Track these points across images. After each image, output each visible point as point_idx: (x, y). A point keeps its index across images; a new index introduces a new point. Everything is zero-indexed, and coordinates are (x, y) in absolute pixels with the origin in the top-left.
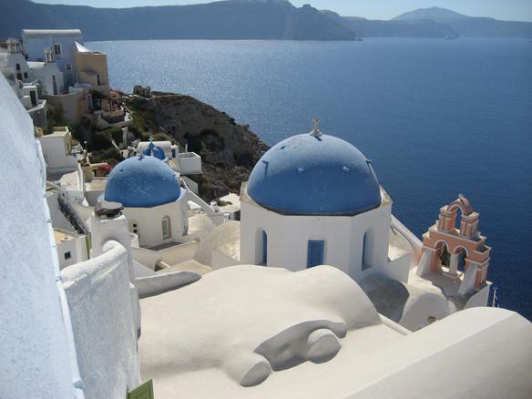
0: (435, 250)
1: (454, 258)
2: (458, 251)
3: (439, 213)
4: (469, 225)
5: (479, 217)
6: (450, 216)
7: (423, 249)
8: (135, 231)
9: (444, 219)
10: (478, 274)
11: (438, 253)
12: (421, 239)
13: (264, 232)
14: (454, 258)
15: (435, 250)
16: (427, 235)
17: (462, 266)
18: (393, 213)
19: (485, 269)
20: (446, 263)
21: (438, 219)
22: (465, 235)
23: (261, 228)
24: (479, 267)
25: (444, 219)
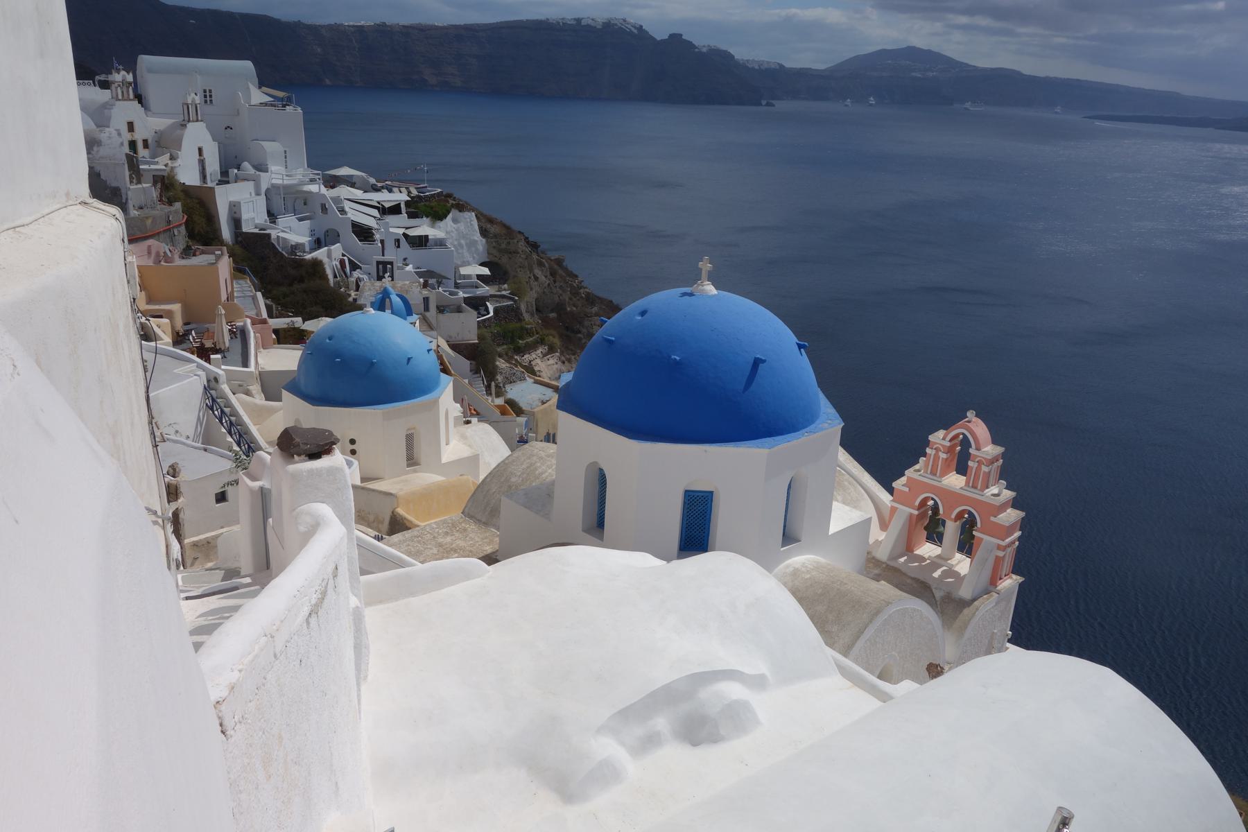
0: (916, 513)
1: (951, 530)
2: (960, 516)
3: (927, 443)
4: (985, 469)
5: (1004, 455)
6: (950, 450)
7: (893, 510)
8: (353, 452)
9: (936, 457)
10: (998, 561)
11: (921, 516)
12: (891, 490)
13: (601, 470)
14: (951, 530)
15: (916, 513)
16: (899, 484)
17: (966, 545)
18: (844, 444)
19: (1009, 557)
20: (935, 535)
21: (925, 455)
22: (974, 487)
23: (596, 463)
24: (999, 547)
25: (936, 457)
